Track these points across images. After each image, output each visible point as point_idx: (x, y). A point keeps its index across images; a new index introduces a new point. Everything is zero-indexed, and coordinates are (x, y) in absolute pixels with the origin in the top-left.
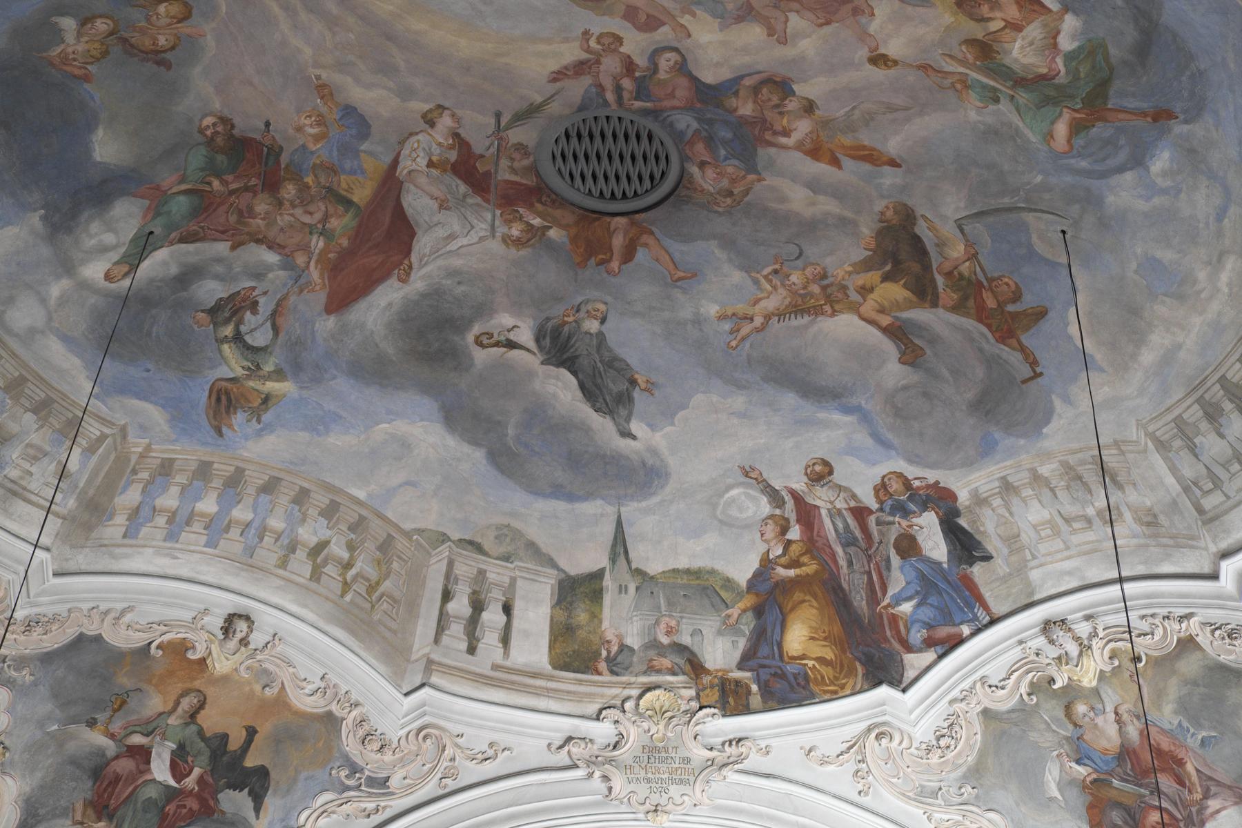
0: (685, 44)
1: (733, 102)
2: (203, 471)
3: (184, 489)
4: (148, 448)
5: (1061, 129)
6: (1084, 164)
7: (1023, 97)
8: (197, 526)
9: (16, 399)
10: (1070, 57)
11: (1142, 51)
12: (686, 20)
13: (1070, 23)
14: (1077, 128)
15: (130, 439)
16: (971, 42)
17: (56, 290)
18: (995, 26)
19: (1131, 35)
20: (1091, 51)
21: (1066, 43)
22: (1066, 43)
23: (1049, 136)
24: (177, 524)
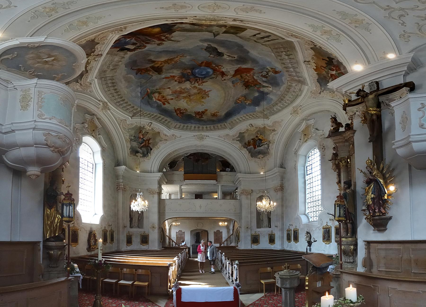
0: (191, 85)
1: (185, 80)
2: (287, 71)
3: (291, 73)
4: (288, 78)
5: (149, 91)
6: (145, 89)
7: (154, 91)
8: (296, 70)
9: (289, 92)
10: (153, 97)
11: (148, 102)
12: (190, 87)
13: (155, 100)
14: (148, 92)
15: (288, 80)
16: (161, 93)
17: (274, 91)
18: (160, 96)
19: (150, 103)
20: (152, 99)
21: (154, 98)
22: (154, 98)
23: (149, 89)
24: (296, 72)
